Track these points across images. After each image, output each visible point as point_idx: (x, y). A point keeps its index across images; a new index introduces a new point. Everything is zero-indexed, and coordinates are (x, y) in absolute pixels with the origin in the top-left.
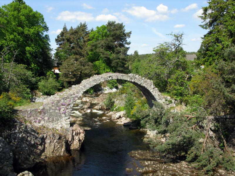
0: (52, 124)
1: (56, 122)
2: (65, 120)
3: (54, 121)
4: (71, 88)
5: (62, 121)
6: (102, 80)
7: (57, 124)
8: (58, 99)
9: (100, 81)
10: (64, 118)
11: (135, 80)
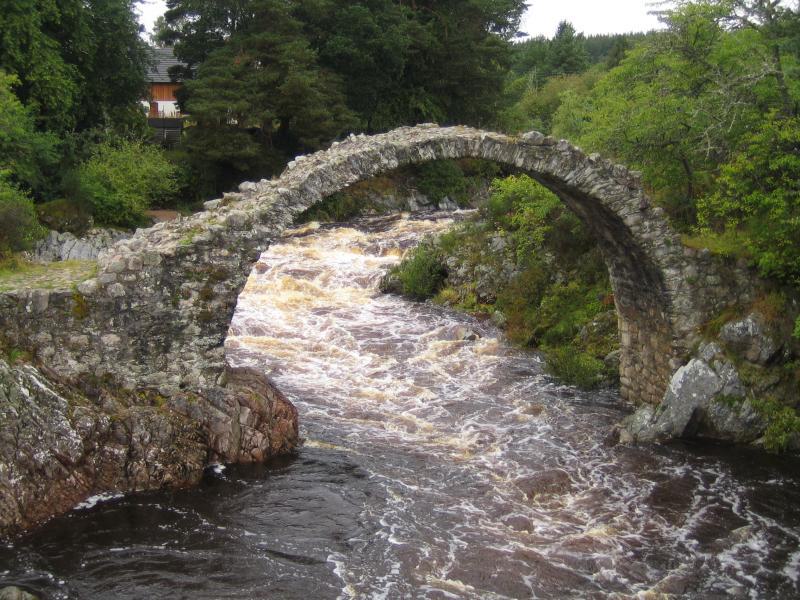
0: (138, 368)
1: (160, 360)
2: (202, 353)
3: (146, 353)
4: (235, 195)
5: (187, 355)
6: (385, 161)
7: (161, 369)
8: (168, 248)
9: (376, 167)
10: (196, 340)
11: (554, 162)
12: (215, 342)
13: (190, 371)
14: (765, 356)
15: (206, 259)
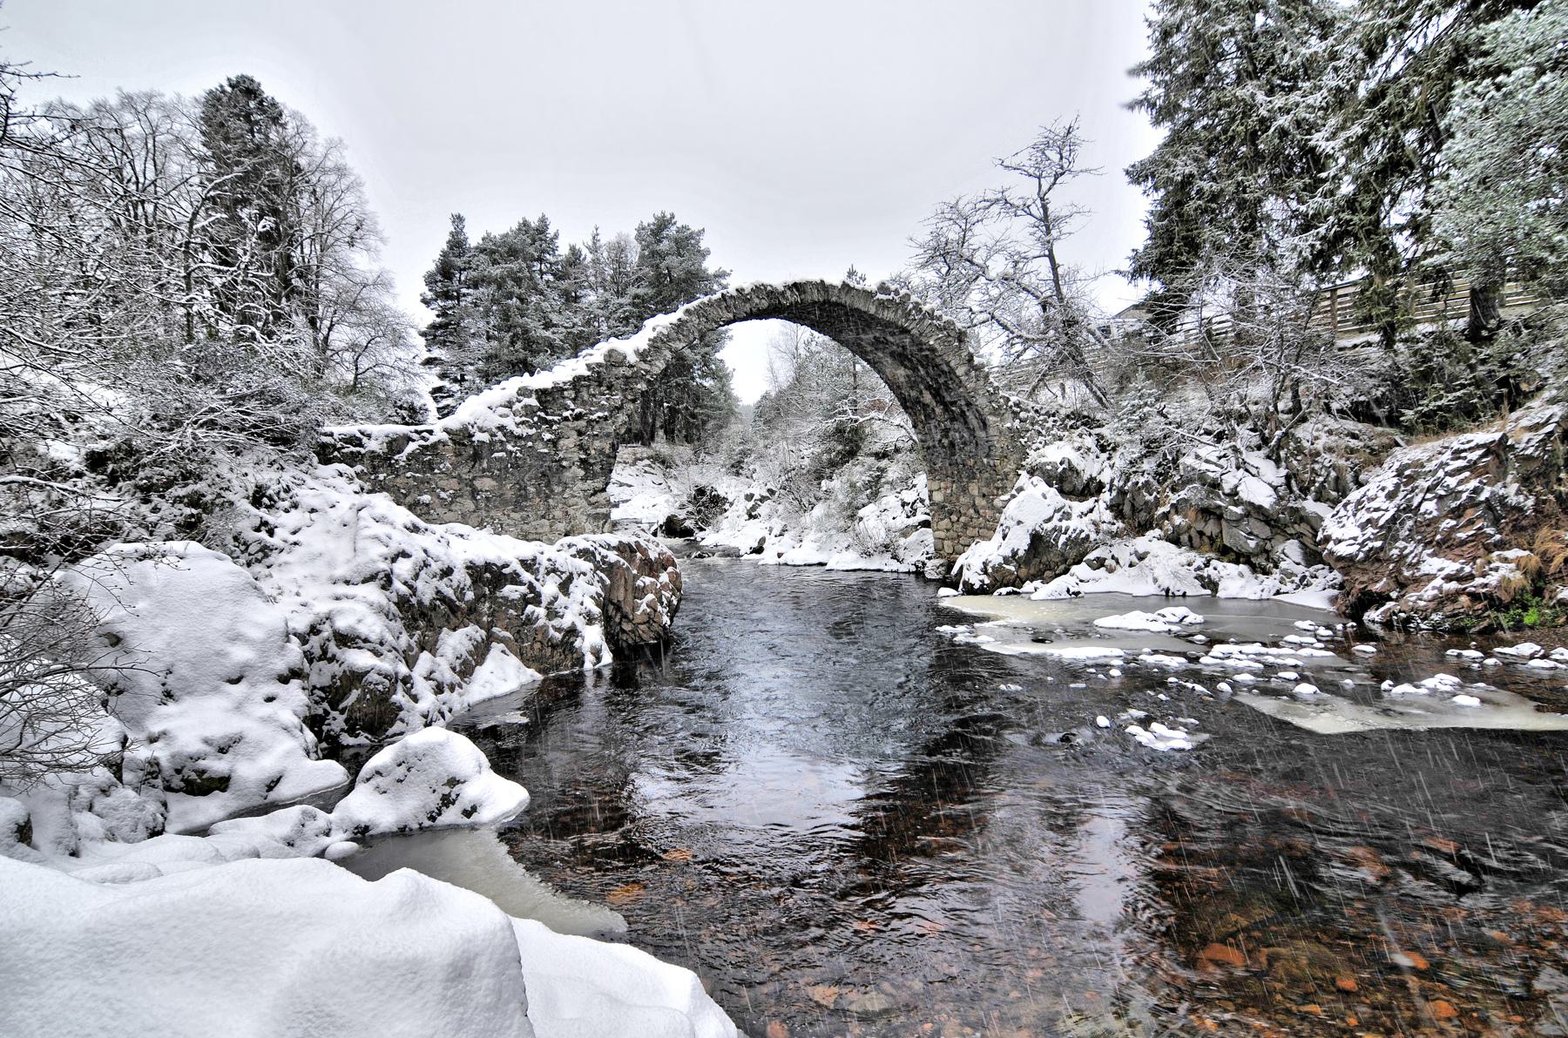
3: (526, 498)
5: (571, 501)
7: (543, 517)
12: (600, 485)
13: (575, 518)
14: (1080, 488)
15: (586, 397)
